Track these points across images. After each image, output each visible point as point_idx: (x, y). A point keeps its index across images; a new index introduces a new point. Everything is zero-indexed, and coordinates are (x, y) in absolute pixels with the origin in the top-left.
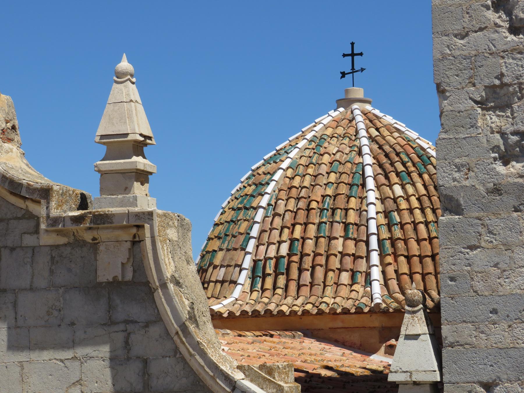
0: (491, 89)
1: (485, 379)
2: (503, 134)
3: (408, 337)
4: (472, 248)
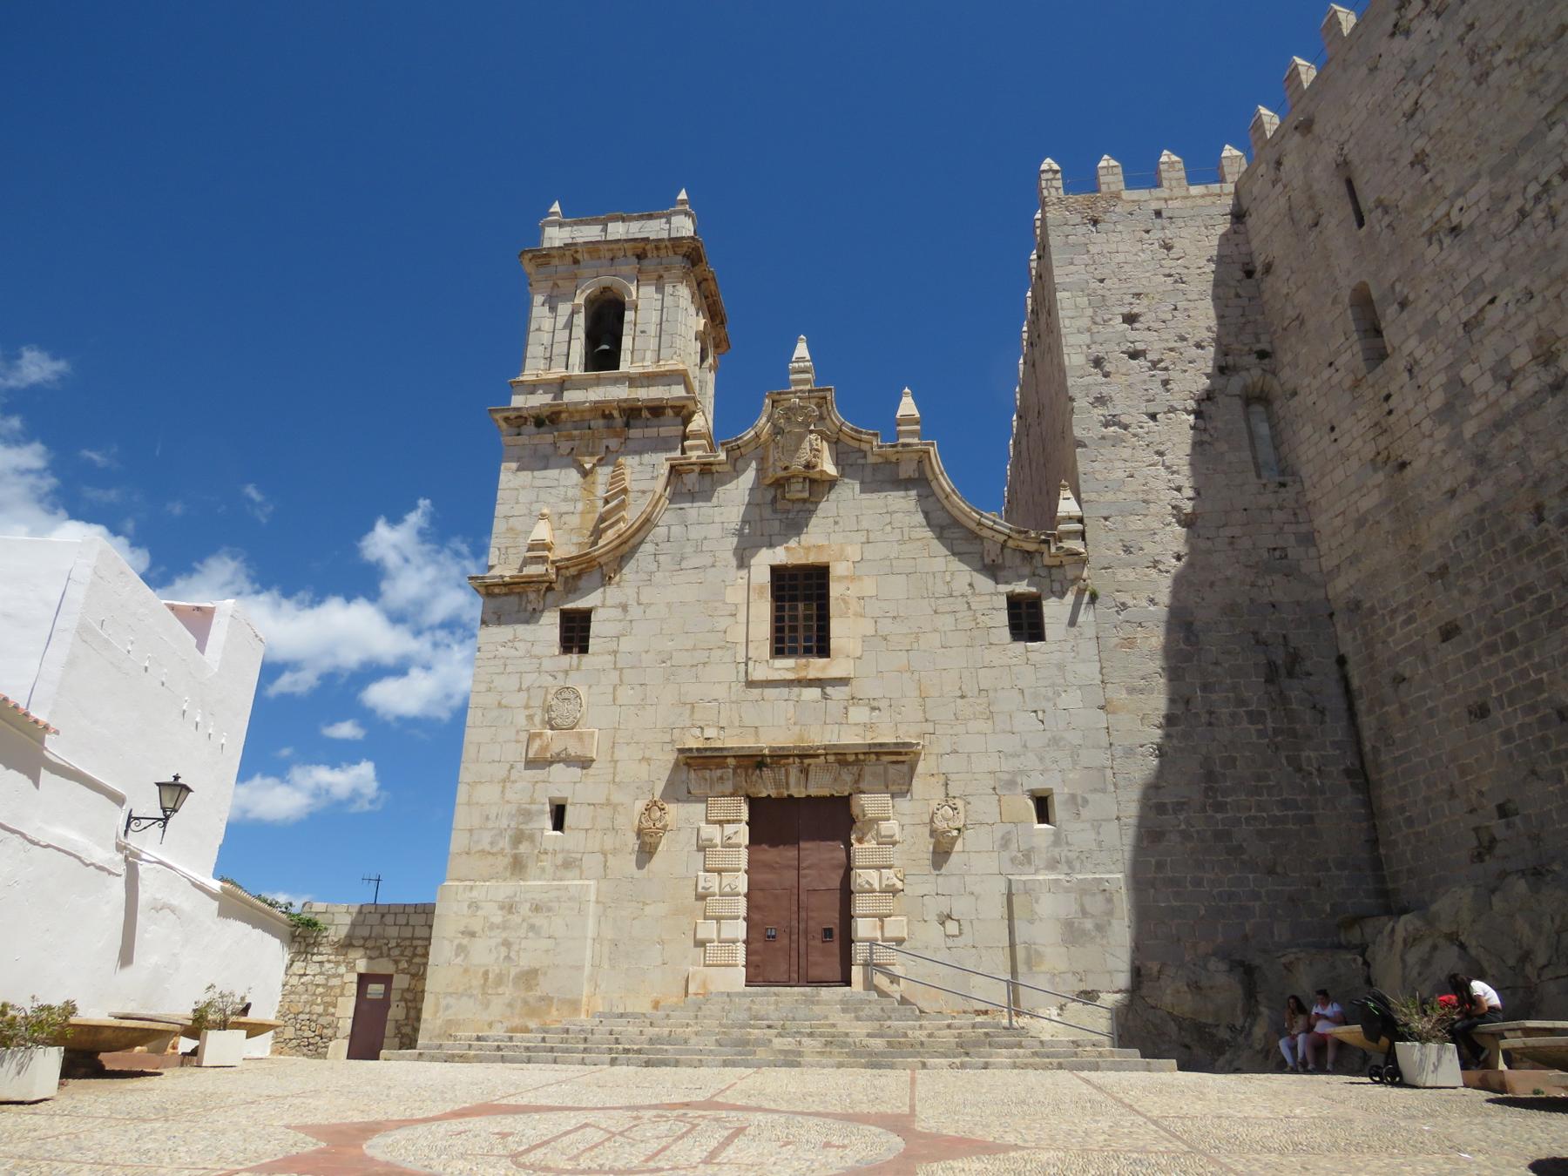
0: (1097, 399)
2: (1104, 416)
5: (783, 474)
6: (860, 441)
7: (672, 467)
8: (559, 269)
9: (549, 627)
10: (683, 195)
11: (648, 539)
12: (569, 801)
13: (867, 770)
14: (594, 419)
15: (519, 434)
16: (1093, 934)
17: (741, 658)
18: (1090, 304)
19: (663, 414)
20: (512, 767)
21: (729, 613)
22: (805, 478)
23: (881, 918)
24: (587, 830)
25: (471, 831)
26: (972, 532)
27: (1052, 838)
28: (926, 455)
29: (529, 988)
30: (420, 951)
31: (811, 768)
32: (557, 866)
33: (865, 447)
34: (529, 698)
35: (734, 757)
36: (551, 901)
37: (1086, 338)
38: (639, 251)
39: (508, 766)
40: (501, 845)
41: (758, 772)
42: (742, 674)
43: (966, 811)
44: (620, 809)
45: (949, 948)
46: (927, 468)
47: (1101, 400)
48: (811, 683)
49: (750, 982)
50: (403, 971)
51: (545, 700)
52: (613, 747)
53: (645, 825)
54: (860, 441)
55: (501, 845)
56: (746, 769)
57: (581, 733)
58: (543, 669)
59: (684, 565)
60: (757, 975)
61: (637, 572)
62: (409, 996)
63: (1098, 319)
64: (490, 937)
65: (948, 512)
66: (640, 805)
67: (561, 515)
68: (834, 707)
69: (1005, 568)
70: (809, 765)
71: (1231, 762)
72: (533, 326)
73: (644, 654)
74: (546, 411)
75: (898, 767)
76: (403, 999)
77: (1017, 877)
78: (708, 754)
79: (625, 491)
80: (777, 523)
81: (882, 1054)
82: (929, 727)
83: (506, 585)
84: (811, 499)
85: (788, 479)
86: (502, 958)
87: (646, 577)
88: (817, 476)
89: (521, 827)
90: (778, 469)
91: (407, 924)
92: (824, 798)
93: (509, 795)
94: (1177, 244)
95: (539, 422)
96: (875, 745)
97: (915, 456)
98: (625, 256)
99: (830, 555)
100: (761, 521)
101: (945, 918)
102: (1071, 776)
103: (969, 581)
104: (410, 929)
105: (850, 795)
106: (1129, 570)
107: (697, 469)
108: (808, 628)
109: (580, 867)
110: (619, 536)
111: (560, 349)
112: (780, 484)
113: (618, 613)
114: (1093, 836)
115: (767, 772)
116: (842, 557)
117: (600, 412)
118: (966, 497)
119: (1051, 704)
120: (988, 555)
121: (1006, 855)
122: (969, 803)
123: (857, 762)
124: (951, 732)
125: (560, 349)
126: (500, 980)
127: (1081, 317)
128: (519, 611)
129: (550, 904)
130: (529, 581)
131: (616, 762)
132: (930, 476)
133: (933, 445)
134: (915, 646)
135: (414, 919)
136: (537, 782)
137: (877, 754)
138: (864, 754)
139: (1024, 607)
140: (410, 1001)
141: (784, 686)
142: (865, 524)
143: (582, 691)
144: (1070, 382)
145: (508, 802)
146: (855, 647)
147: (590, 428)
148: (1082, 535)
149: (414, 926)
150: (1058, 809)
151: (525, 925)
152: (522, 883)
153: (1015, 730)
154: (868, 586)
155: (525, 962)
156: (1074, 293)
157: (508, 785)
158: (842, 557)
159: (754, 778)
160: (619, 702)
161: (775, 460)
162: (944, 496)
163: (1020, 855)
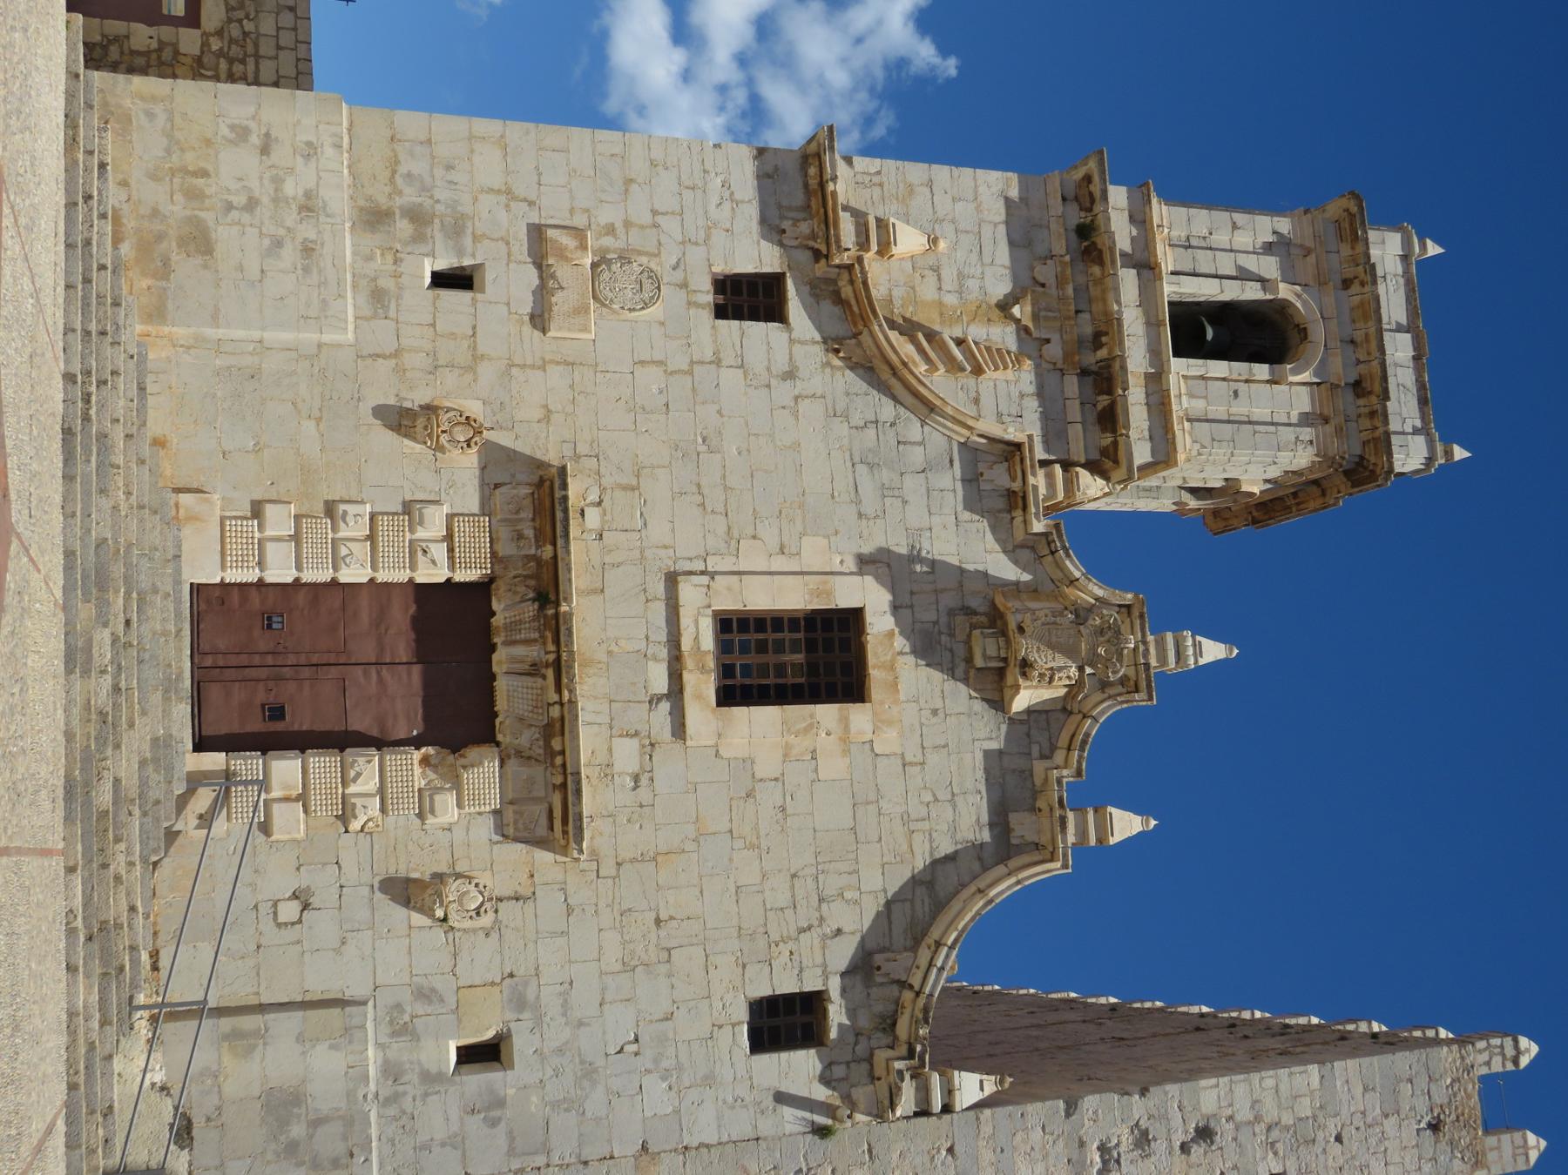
0: (1145, 1133)
1: (956, 1148)
2: (1118, 1145)
3: (981, 1082)
4: (1043, 1128)
5: (1012, 625)
6: (1069, 749)
7: (1018, 446)
8: (1334, 257)
10: (1459, 453)
11: (902, 410)
12: (479, 296)
13: (538, 771)
14: (1093, 319)
15: (1064, 199)
16: (282, 1138)
17: (713, 564)
18: (1301, 1119)
19: (1104, 430)
20: (531, 204)
21: (786, 542)
22: (1005, 660)
23: (303, 798)
24: (433, 325)
25: (429, 141)
26: (924, 933)
27: (434, 1070)
28: (1049, 856)
29: (182, 243)
30: (238, 68)
31: (540, 680)
32: (375, 279)
33: (1059, 757)
34: (642, 227)
35: (555, 557)
36: (320, 272)
37: (1244, 1114)
38: (1367, 385)
39: (533, 197)
40: (407, 190)
41: (531, 595)
42: (688, 566)
43: (474, 931)
44: (469, 377)
45: (256, 907)
46: (1025, 859)
47: (1143, 1139)
48: (676, 677)
49: (197, 589)
50: (205, 45)
51: (640, 253)
52: (566, 363)
53: (444, 417)
54: (1069, 749)
55: (407, 190)
56: (537, 576)
57: (587, 311)
58: (690, 249)
59: (862, 469)
61: (848, 394)
62: (167, 54)
63: (1275, 1134)
64: (261, 178)
65: (957, 893)
66: (474, 408)
67: (936, 270)
68: (637, 716)
69: (868, 987)
70: (544, 677)
72: (1240, 218)
73: (717, 408)
74: (1101, 241)
75: (544, 821)
76: (162, 45)
77: (370, 1015)
78: (559, 515)
79: (978, 371)
80: (934, 618)
81: (87, 803)
82: (608, 869)
83: (822, 185)
84: (972, 672)
85: (1004, 633)
86: (231, 198)
87: (840, 406)
88: (1009, 680)
89: (437, 221)
90: (1019, 617)
91: (279, 48)
92: (491, 701)
93: (487, 201)
95: (1085, 231)
96: (578, 783)
97: (1045, 839)
98: (1359, 362)
99: (882, 703)
101: (303, 899)
102: (534, 1099)
103: (846, 929)
104: (272, 53)
105: (498, 744)
107: (1016, 486)
108: (763, 670)
109: (375, 316)
110: (905, 364)
111: (1205, 262)
112: (995, 620)
113: (781, 364)
114: (440, 1135)
115: (530, 609)
117: (1103, 328)
118: (981, 921)
119: (650, 1066)
120: (888, 960)
121: (406, 996)
122: (487, 935)
123: (551, 754)
124: (602, 905)
125: (1205, 262)
126: (195, 195)
127: (1279, 1107)
128: (780, 207)
129: (315, 270)
130: (828, 222)
131: (543, 368)
132: (1013, 863)
133: (1065, 866)
134: (739, 844)
135: (287, 58)
136: (508, 243)
137: (564, 785)
138: (564, 765)
139: (806, 1019)
140: (159, 57)
141: (669, 633)
142: (933, 759)
143: (655, 311)
144: (1173, 1089)
145: (476, 199)
146: (735, 745)
147: (1077, 312)
148: (923, 1112)
149: (276, 58)
150: (479, 1079)
151: (282, 232)
152: (348, 225)
153: (606, 1007)
154: (833, 766)
155: (224, 235)
156: (1317, 1094)
157: (503, 198)
159: (522, 589)
160: (639, 371)
161: (1033, 611)
162: (982, 885)
163: (407, 1018)
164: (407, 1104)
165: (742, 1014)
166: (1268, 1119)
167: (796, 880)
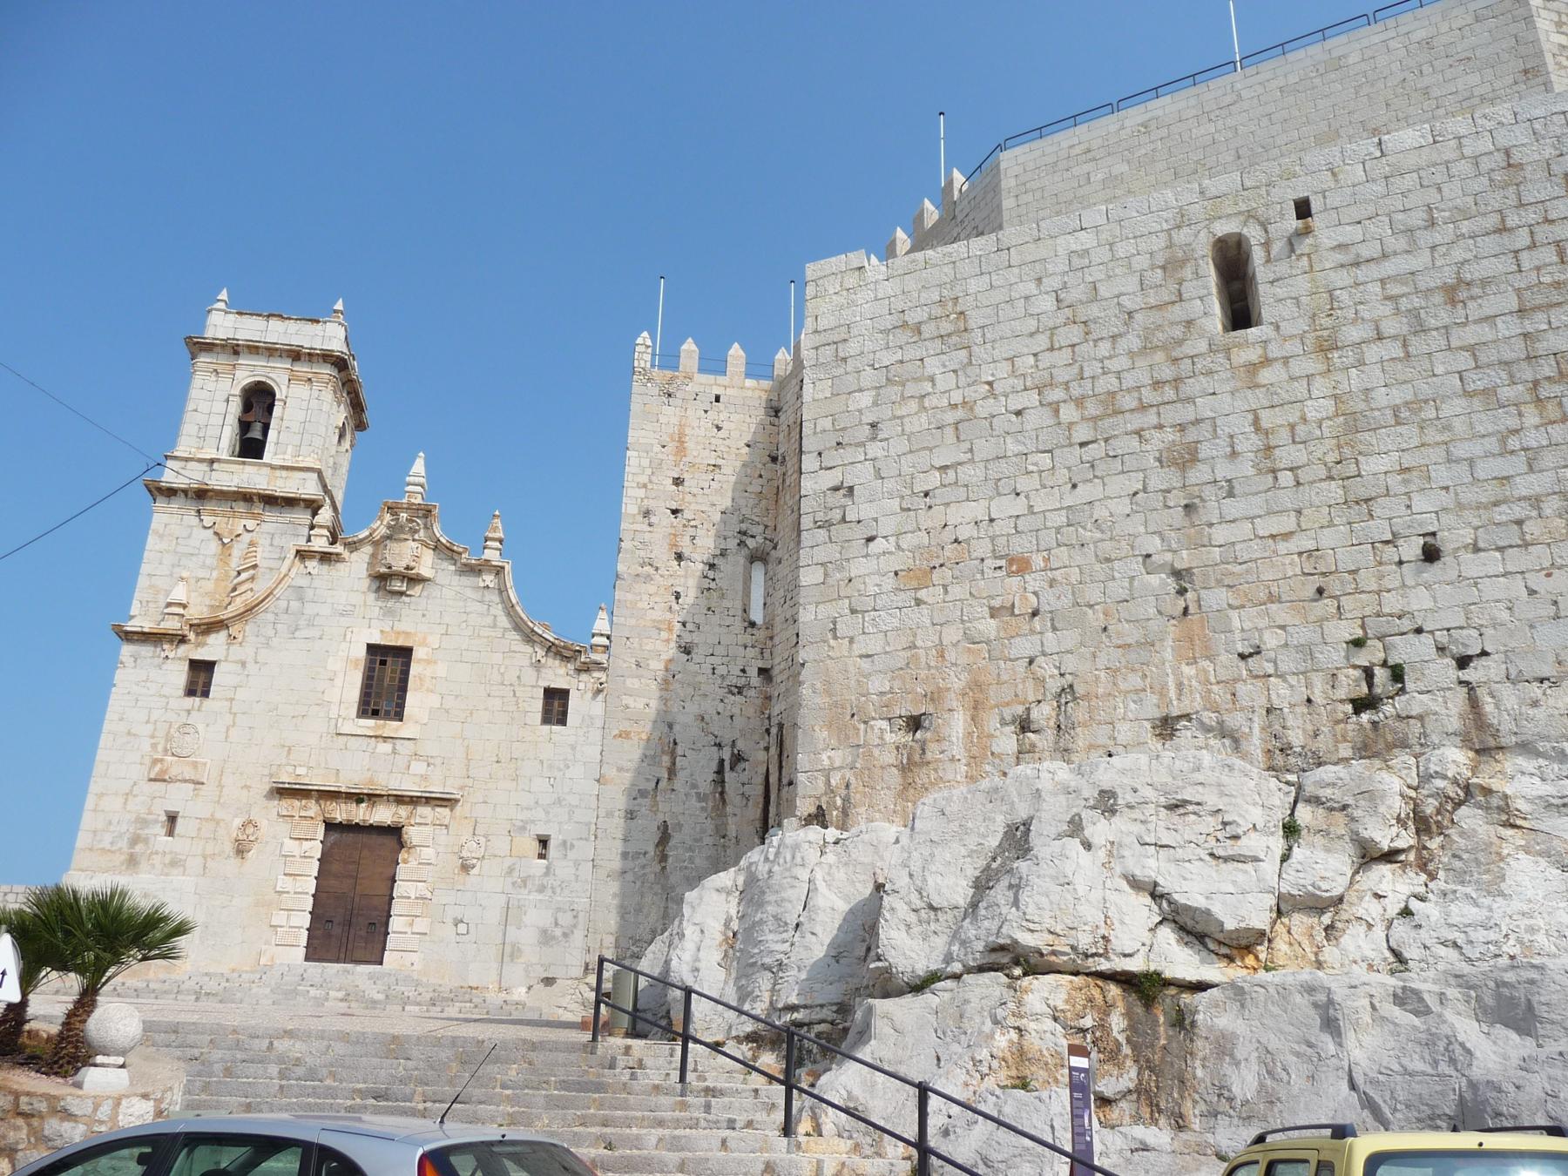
7: (298, 552)
9: (179, 675)
10: (339, 306)
20: (135, 784)
25: (95, 832)
48: (385, 738)
49: (307, 959)
53: (241, 837)
55: (119, 845)
59: (297, 634)
60: (315, 952)
66: (238, 822)
67: (198, 580)
71: (680, 826)
72: (191, 406)
82: (469, 782)
87: (262, 640)
94: (725, 425)
100: (365, 605)
106: (636, 680)
107: (318, 556)
116: (424, 644)
121: (510, 880)
134: (469, 719)
143: (201, 727)
144: (623, 526)
157: (130, 797)
158: (424, 644)
164: (556, 884)
165: (547, 728)
166: (646, 481)
167: (492, 693)
